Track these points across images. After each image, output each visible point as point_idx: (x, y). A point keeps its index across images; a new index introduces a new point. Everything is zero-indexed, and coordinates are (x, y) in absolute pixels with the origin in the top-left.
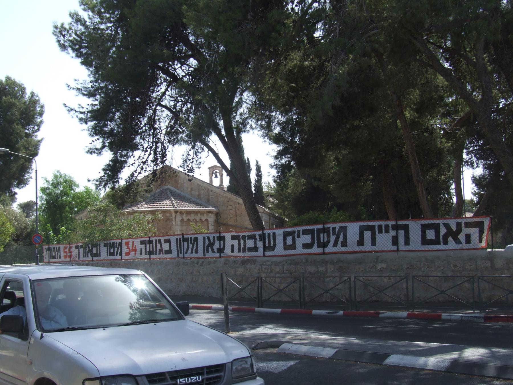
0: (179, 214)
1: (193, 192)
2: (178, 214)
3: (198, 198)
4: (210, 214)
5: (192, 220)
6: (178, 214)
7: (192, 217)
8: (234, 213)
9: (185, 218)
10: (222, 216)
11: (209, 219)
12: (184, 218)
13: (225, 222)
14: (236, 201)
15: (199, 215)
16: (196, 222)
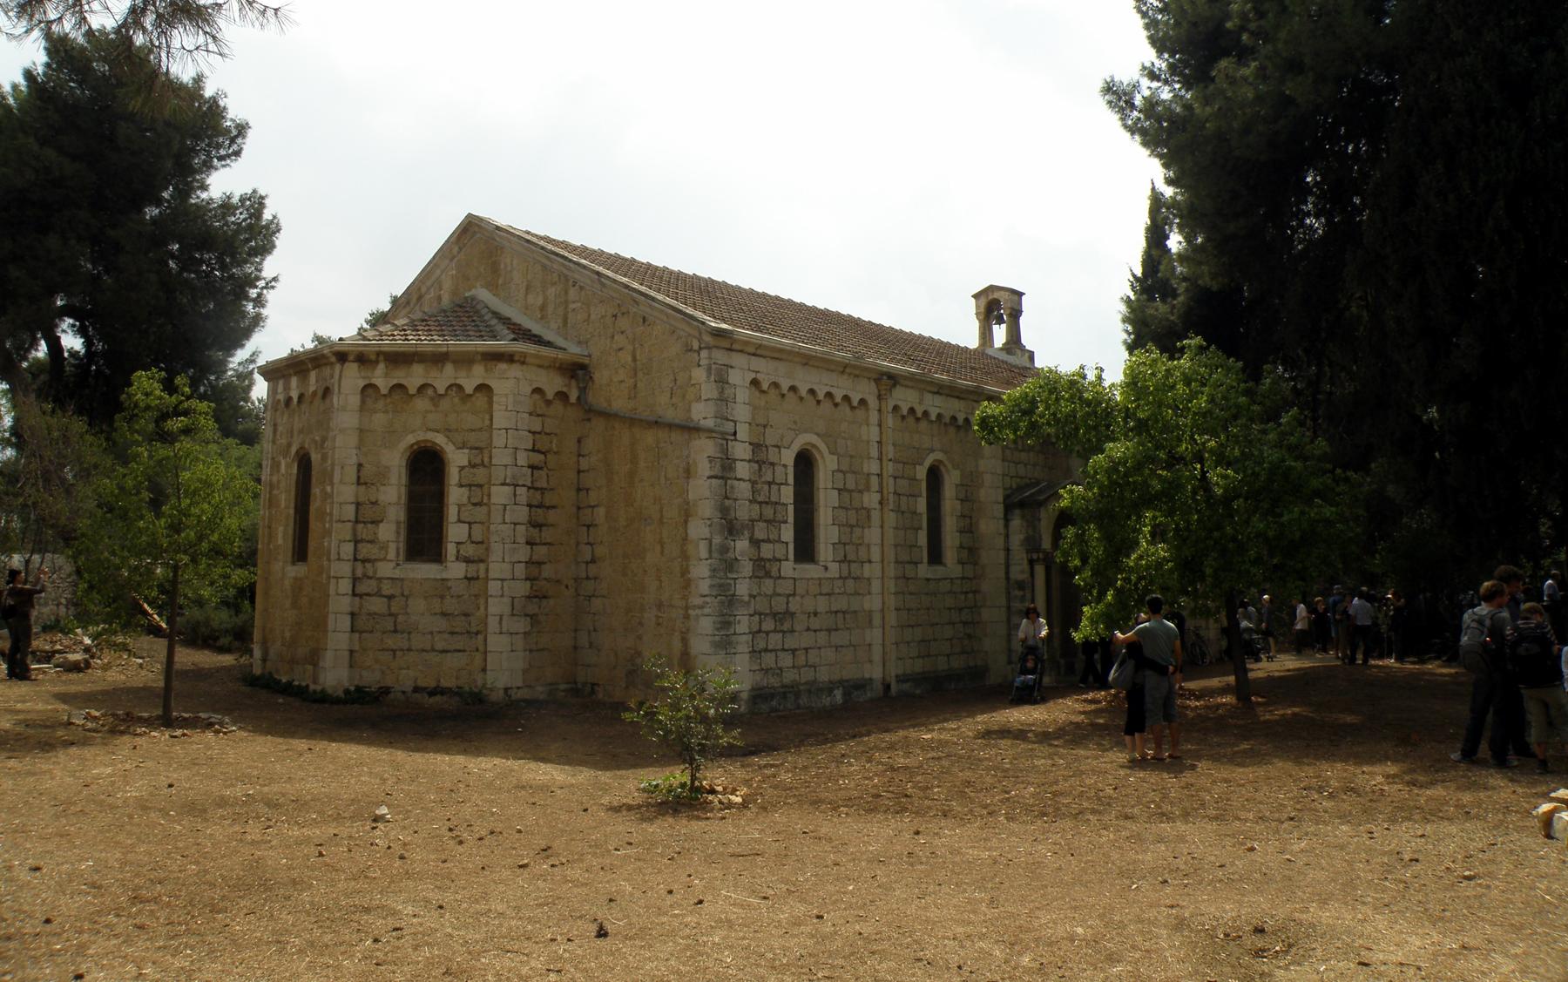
0: (355, 366)
1: (531, 298)
3: (542, 318)
4: (503, 366)
5: (412, 391)
7: (414, 377)
8: (629, 359)
10: (596, 376)
11: (492, 383)
12: (374, 381)
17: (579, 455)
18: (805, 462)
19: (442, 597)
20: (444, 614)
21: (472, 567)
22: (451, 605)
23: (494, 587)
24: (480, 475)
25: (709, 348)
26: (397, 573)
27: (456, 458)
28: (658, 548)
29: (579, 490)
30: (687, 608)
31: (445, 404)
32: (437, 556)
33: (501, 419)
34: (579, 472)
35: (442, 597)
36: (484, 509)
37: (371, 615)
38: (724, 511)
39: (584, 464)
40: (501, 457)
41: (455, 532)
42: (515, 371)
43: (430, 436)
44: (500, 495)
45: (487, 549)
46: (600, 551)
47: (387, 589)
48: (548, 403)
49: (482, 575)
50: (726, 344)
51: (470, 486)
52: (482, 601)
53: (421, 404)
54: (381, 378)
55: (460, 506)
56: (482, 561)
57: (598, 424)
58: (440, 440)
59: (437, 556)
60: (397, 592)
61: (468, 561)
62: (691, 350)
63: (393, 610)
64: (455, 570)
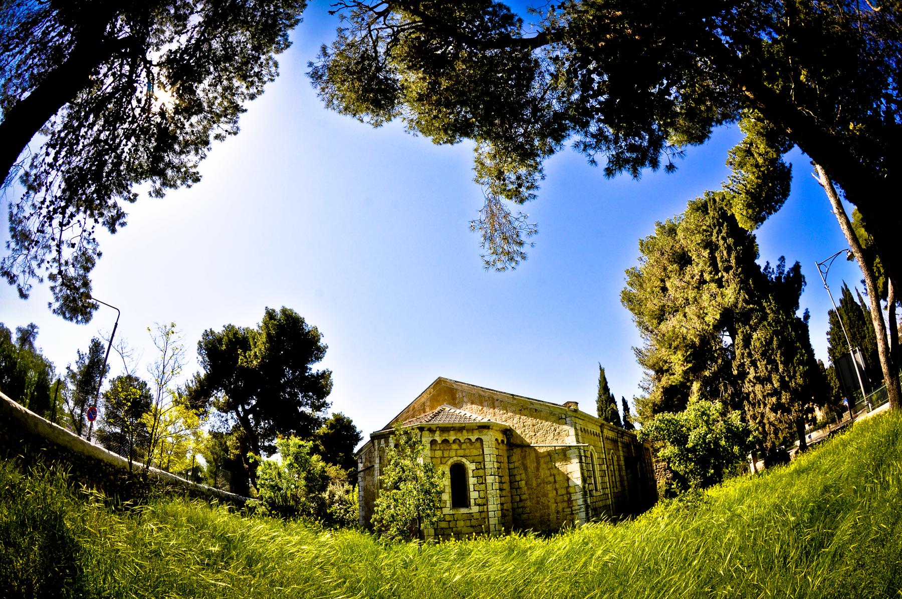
0: (427, 433)
2: (426, 433)
4: (486, 430)
6: (426, 433)
7: (452, 437)
9: (438, 438)
11: (483, 437)
13: (519, 442)
14: (531, 406)
15: (465, 432)
16: (460, 444)
17: (508, 463)
18: (591, 455)
19: (471, 520)
20: (471, 526)
21: (481, 507)
22: (474, 522)
23: (491, 514)
24: (481, 472)
25: (570, 417)
26: (451, 512)
27: (471, 467)
28: (555, 492)
29: (510, 476)
30: (572, 511)
31: (464, 446)
32: (467, 505)
33: (486, 451)
34: (509, 469)
35: (471, 520)
36: (484, 485)
37: (442, 529)
38: (582, 474)
39: (512, 466)
40: (488, 465)
41: (473, 495)
42: (491, 432)
43: (459, 458)
44: (490, 479)
45: (487, 500)
46: (524, 497)
47: (448, 518)
48: (499, 444)
49: (485, 510)
50: (574, 414)
51: (477, 477)
52: (486, 520)
53: (455, 446)
54: (438, 438)
55: (474, 485)
56: (484, 505)
57: (517, 451)
58: (464, 460)
59: (467, 505)
60: (452, 519)
61: (479, 505)
62: (562, 418)
63: (451, 526)
64: (475, 509)
